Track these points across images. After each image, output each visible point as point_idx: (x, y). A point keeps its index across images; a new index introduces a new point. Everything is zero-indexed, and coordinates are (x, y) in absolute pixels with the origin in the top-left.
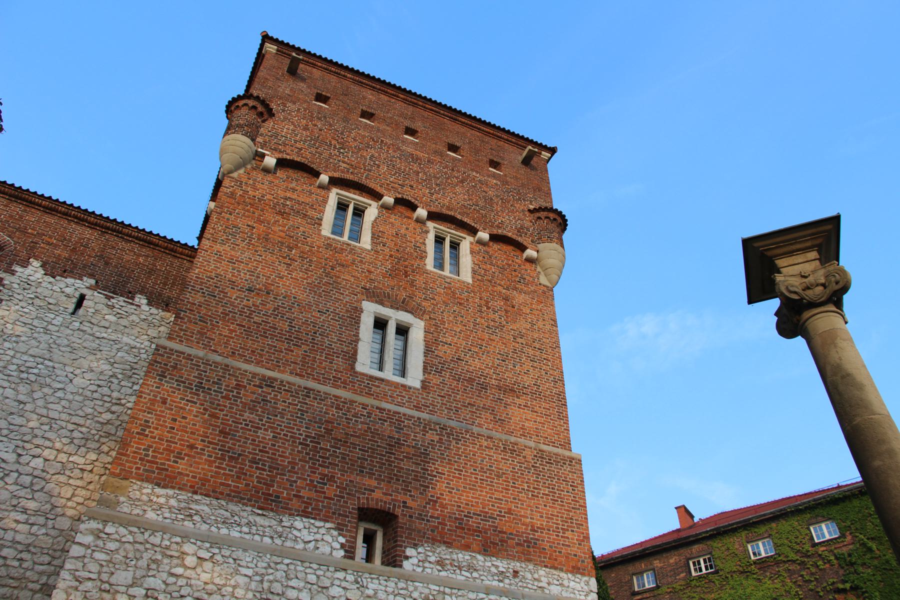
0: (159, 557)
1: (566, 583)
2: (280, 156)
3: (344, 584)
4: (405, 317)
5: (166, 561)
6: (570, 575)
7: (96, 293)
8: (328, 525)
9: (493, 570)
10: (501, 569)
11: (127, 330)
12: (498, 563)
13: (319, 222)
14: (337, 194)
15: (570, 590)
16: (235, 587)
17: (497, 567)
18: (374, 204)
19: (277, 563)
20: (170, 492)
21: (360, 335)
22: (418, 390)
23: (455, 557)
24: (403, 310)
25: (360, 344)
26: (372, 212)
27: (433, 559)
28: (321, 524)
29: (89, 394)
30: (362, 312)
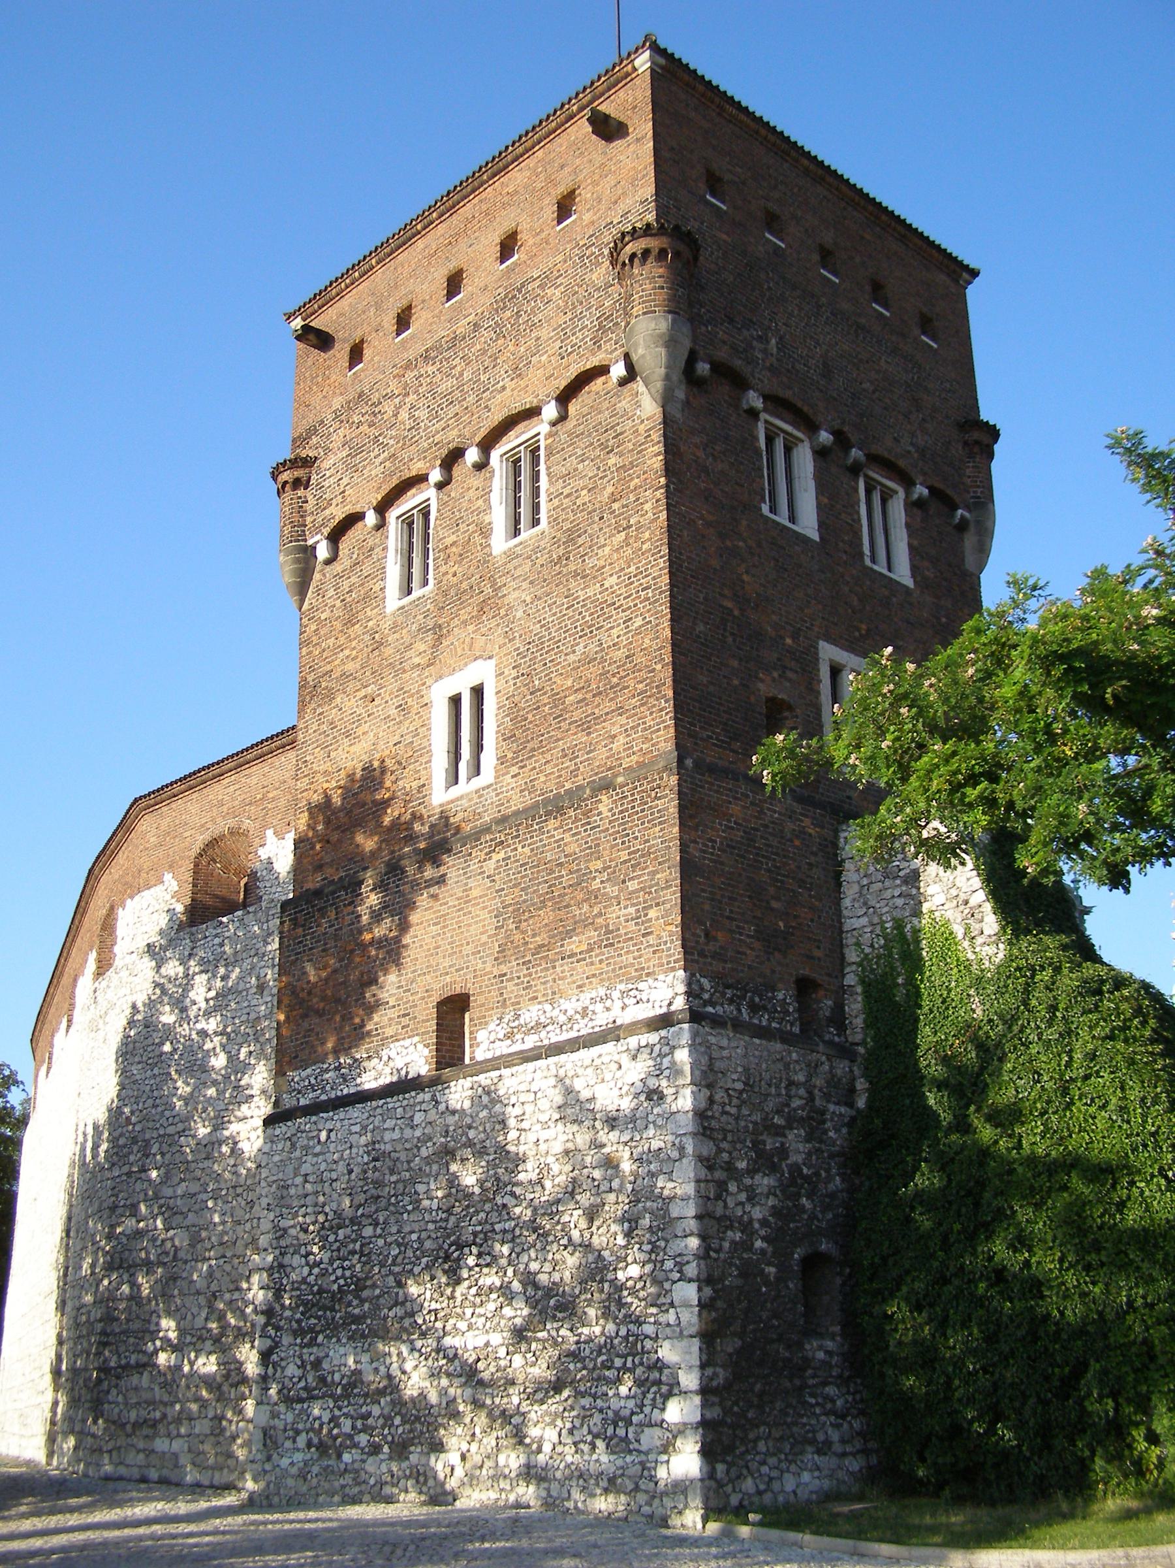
0: (306, 1142)
2: (326, 531)
3: (424, 1107)
5: (311, 1143)
8: (416, 1039)
12: (565, 1005)
14: (398, 518)
16: (351, 1148)
19: (375, 1109)
20: (309, 1071)
22: (491, 785)
27: (501, 1036)
28: (407, 1042)
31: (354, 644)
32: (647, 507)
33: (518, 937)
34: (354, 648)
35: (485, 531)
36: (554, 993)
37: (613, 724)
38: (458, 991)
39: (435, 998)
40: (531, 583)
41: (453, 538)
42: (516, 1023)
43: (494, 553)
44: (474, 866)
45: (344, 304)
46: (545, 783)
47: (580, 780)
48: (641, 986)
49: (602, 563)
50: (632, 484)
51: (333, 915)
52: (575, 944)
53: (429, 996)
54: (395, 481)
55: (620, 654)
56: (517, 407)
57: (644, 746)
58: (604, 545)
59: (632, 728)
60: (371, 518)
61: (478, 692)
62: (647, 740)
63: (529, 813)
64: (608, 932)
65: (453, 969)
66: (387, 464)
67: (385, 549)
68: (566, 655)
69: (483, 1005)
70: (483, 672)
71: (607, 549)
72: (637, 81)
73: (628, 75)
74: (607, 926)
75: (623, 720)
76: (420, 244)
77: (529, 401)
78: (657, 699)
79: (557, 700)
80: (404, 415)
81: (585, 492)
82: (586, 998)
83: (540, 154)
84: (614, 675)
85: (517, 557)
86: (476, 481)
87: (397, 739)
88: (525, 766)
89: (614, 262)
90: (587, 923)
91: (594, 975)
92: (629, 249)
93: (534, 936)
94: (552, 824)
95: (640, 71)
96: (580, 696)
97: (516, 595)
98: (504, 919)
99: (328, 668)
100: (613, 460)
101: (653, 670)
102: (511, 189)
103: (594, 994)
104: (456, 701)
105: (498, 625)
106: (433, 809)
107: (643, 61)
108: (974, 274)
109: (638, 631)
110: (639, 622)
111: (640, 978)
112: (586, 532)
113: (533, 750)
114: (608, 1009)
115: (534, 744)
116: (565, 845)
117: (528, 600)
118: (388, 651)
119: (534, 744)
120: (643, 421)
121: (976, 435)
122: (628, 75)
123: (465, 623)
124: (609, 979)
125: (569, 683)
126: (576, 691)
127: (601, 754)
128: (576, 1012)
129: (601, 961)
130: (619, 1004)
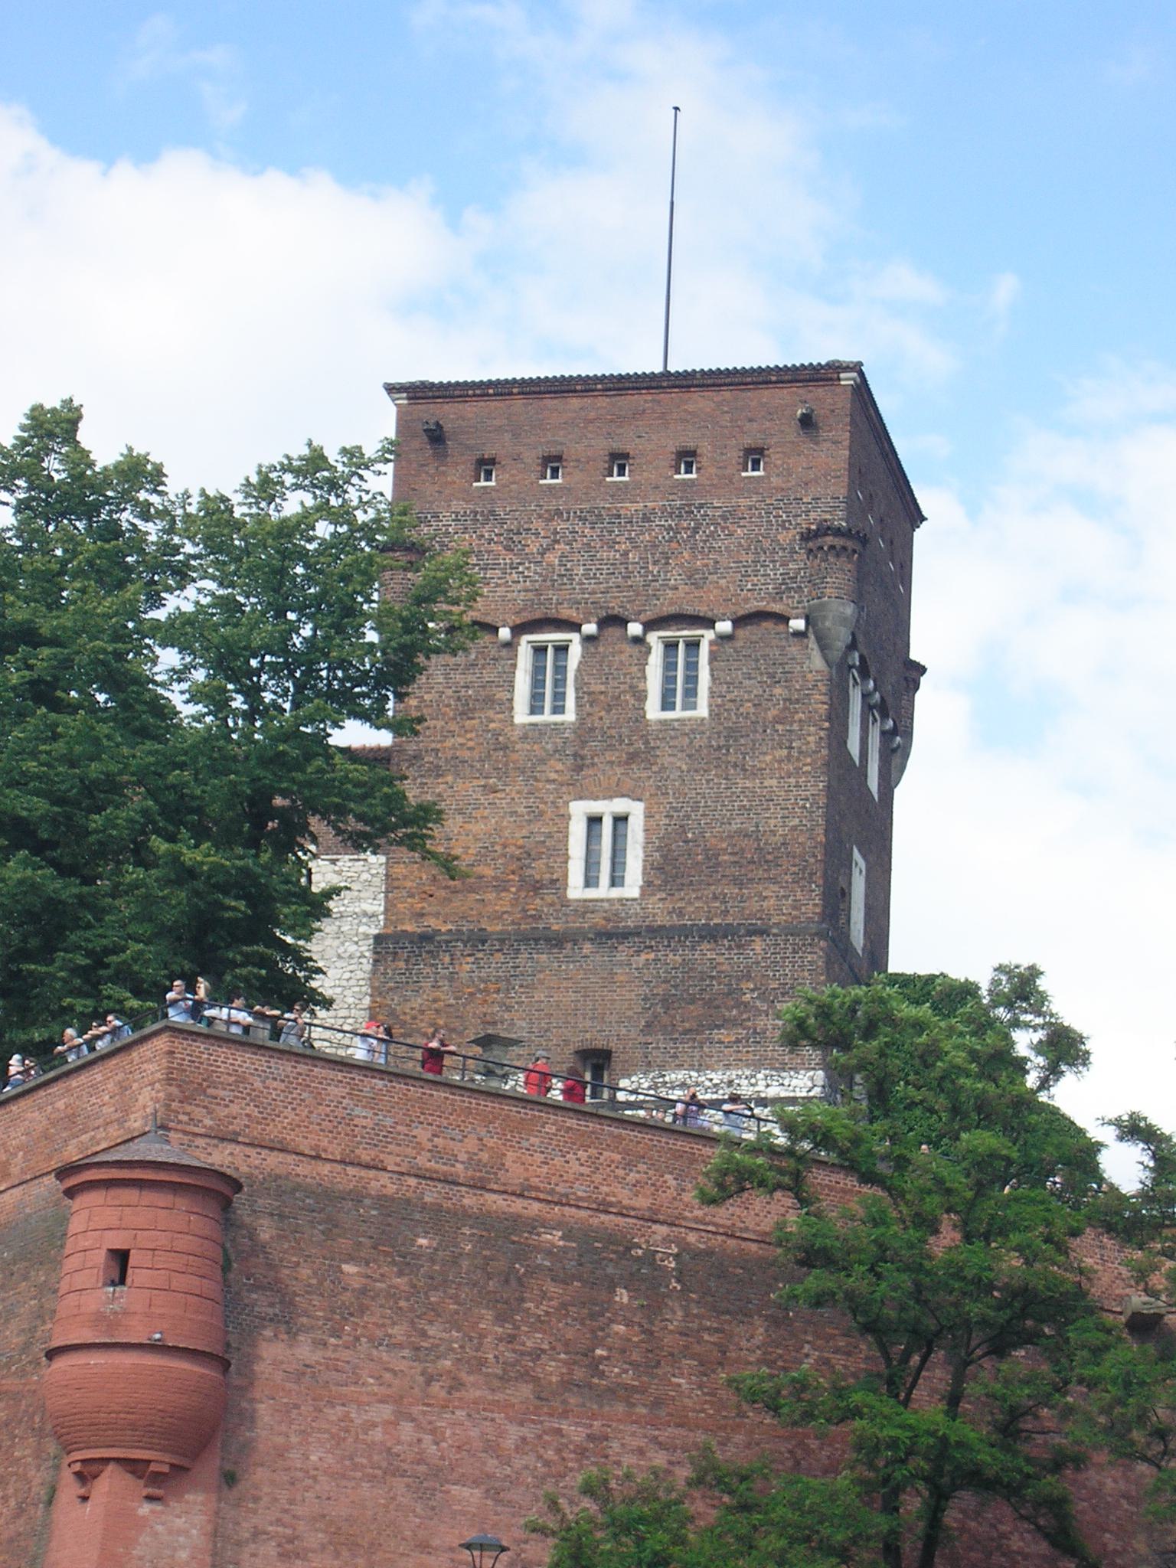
1: (786, 1082)
4: (620, 805)
6: (792, 1073)
7: (321, 862)
9: (708, 1083)
10: (714, 1082)
11: (362, 895)
12: (713, 1075)
13: (509, 706)
14: (529, 642)
15: (791, 1088)
17: (711, 1080)
18: (575, 637)
21: (570, 852)
23: (667, 1079)
24: (617, 796)
25: (570, 862)
26: (576, 651)
27: (646, 1085)
29: (344, 983)
30: (570, 819)
31: (469, 736)
32: (811, 739)
33: (666, 1019)
34: (471, 739)
35: (641, 696)
36: (701, 1065)
37: (766, 888)
38: (600, 1044)
39: (572, 1048)
40: (689, 756)
41: (603, 688)
42: (661, 1080)
43: (649, 716)
44: (621, 957)
45: (471, 409)
46: (693, 912)
47: (729, 920)
48: (784, 1074)
49: (764, 766)
50: (796, 717)
51: (447, 959)
52: (721, 1035)
53: (566, 1045)
54: (538, 615)
55: (779, 840)
56: (689, 610)
57: (794, 913)
58: (765, 754)
59: (784, 896)
60: (505, 633)
61: (621, 820)
62: (795, 908)
63: (684, 932)
64: (755, 1032)
65: (594, 1030)
66: (530, 595)
67: (514, 666)
68: (722, 823)
69: (627, 1061)
70: (636, 810)
71: (768, 758)
72: (838, 390)
73: (831, 379)
74: (755, 1029)
75: (775, 888)
76: (575, 402)
77: (702, 610)
78: (810, 883)
79: (712, 856)
80: (553, 558)
81: (750, 704)
82: (733, 1074)
83: (727, 395)
84: (769, 853)
85: (674, 729)
86: (635, 650)
87: (524, 832)
88: (673, 895)
89: (807, 536)
90: (734, 1023)
91: (741, 1060)
92: (829, 540)
93: (682, 1022)
94: (705, 946)
95: (842, 383)
96: (735, 859)
97: (674, 761)
98: (652, 1004)
99: (433, 745)
100: (777, 691)
101: (806, 861)
102: (691, 407)
103: (740, 1073)
104: (594, 821)
105: (650, 777)
106: (569, 901)
107: (847, 379)
108: (923, 519)
109: (794, 828)
110: (796, 821)
111: (784, 1070)
112: (748, 736)
113: (683, 885)
114: (752, 1085)
115: (686, 881)
116: (718, 964)
117: (684, 767)
118: (514, 756)
119: (686, 881)
120: (811, 672)
121: (914, 674)
122: (831, 379)
123: (611, 763)
124: (754, 1065)
125: (724, 845)
126: (731, 854)
127: (754, 905)
128: (722, 1082)
129: (748, 1052)
130: (762, 1083)
